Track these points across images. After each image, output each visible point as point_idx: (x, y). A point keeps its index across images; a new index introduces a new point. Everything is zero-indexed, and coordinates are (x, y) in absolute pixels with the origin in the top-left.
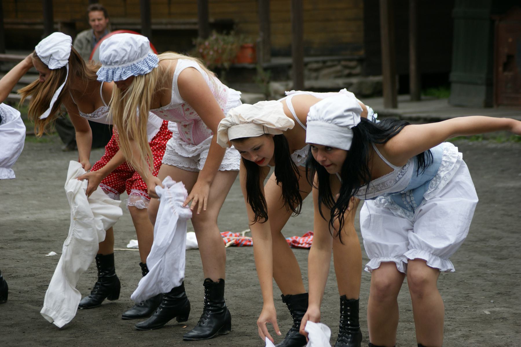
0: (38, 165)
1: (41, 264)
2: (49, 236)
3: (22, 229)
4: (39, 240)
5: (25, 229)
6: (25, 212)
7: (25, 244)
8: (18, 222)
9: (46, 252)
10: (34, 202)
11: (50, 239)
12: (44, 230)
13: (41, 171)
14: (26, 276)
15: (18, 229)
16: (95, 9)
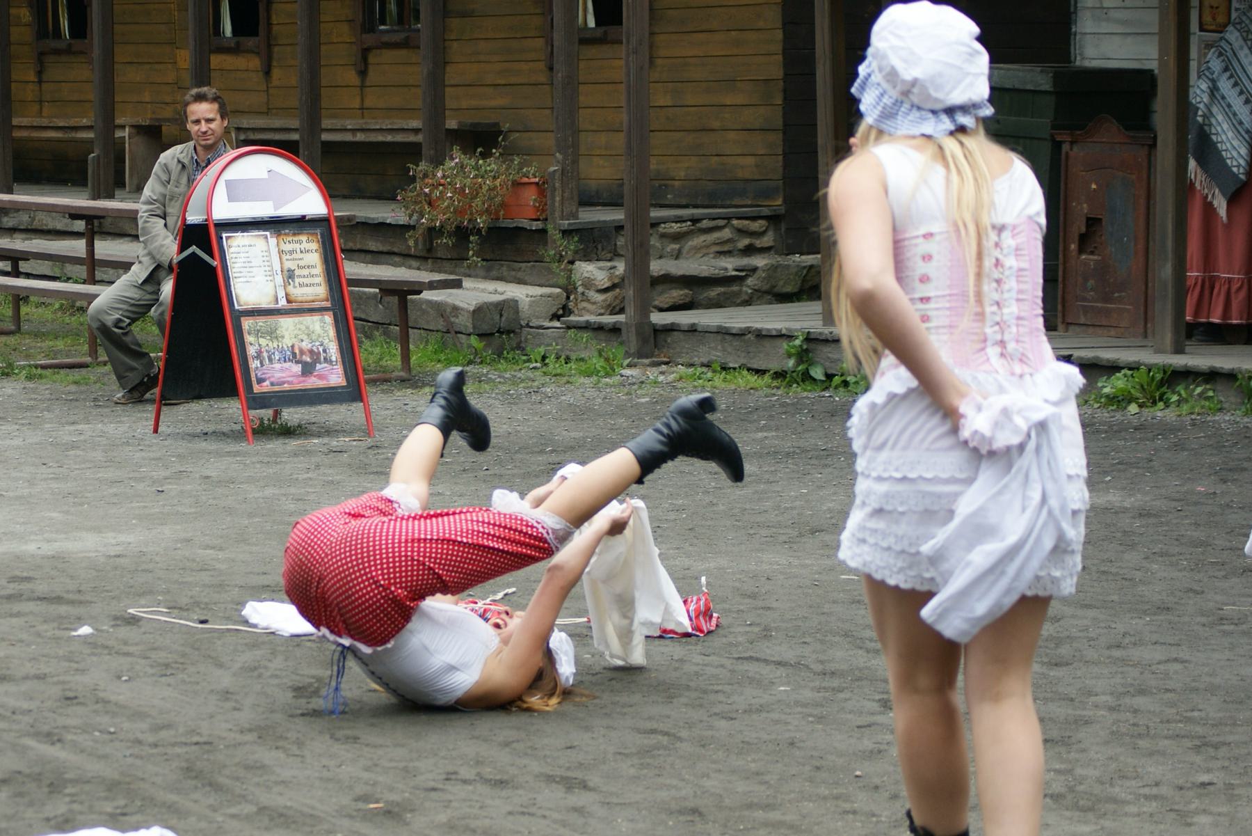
0: (66, 434)
1: (61, 652)
2: (80, 591)
3: (25, 574)
4: (58, 600)
5: (31, 574)
6: (32, 537)
7: (31, 606)
8: (18, 558)
9: (72, 626)
10: (54, 515)
11: (82, 598)
12: (72, 577)
13: (73, 446)
14: (26, 678)
15: (18, 573)
16: (200, 98)
